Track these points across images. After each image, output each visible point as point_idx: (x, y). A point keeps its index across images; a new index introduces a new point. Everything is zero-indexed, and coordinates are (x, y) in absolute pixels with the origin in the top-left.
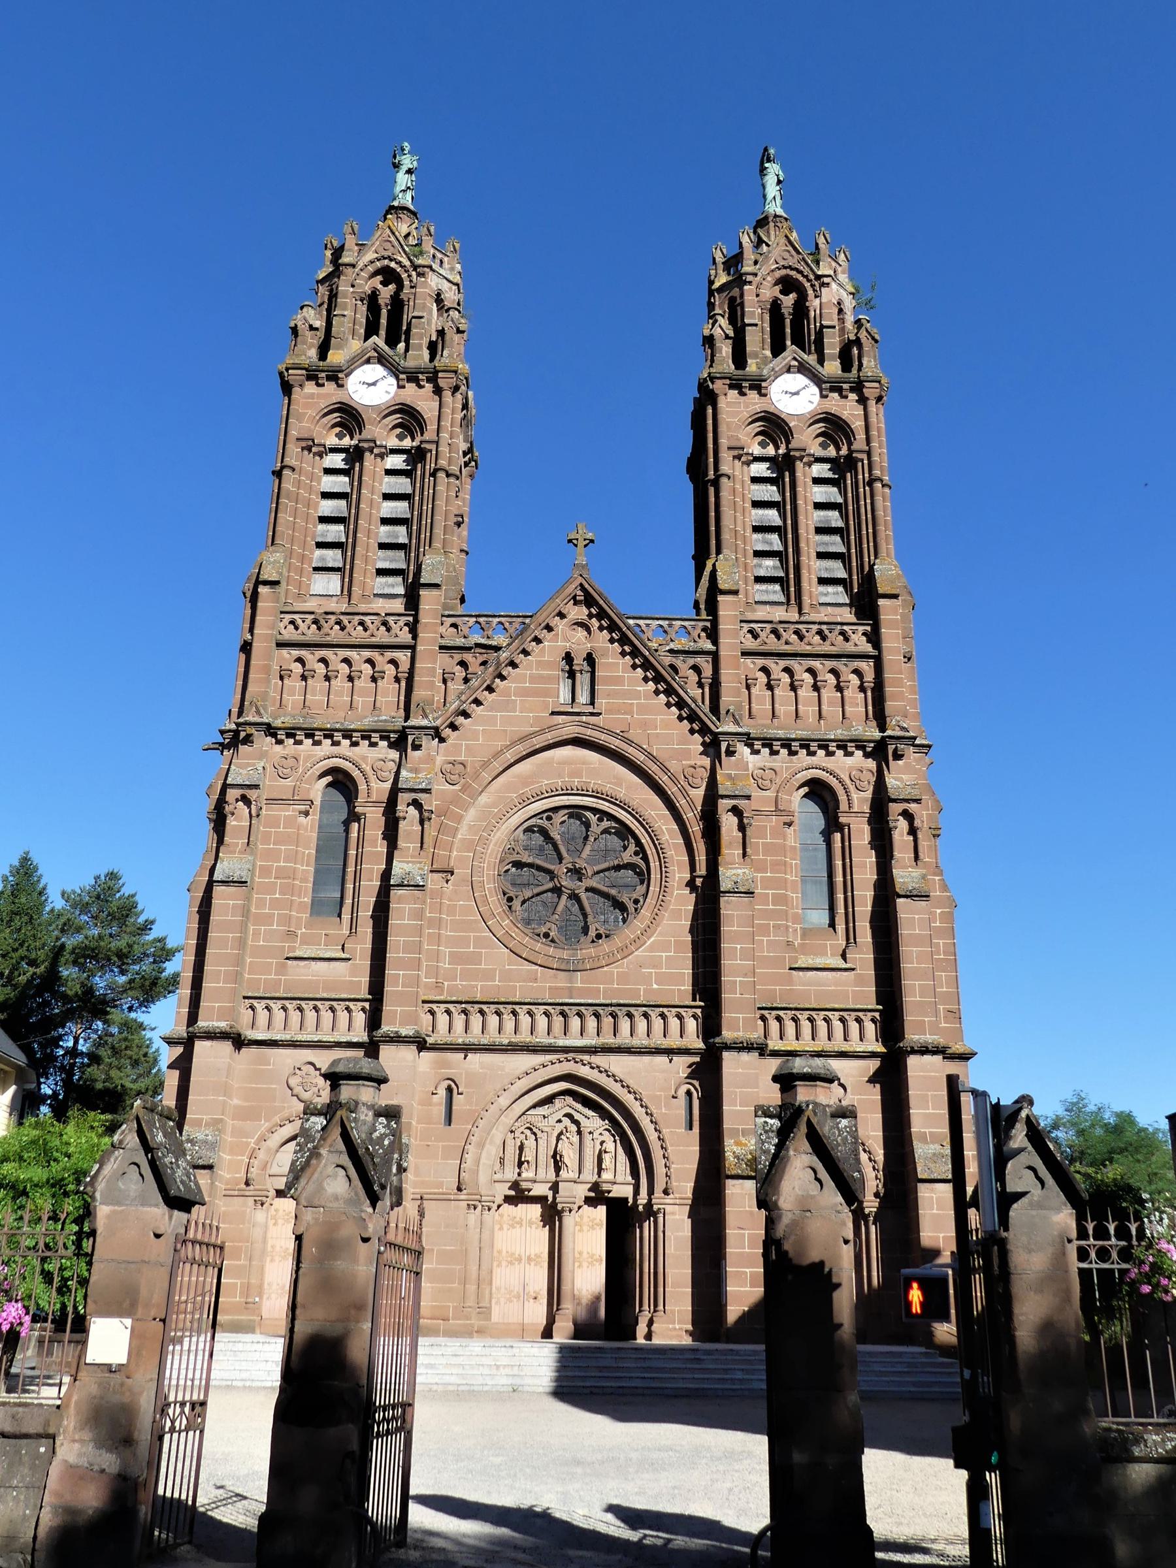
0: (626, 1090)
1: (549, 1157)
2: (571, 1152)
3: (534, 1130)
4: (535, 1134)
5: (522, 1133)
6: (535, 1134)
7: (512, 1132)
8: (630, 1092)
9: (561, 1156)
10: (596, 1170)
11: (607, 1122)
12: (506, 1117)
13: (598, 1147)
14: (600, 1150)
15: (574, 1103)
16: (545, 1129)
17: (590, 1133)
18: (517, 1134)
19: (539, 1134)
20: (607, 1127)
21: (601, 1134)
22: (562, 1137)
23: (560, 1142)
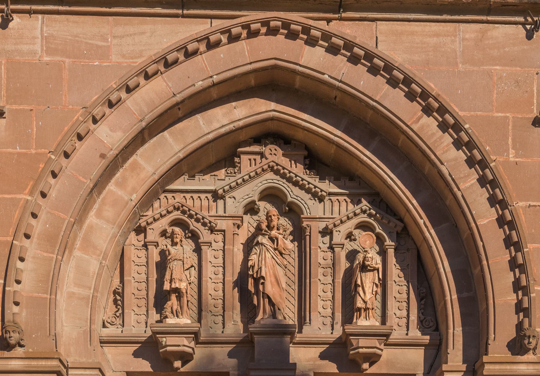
0: (416, 107)
1: (229, 285)
2: (280, 272)
3: (193, 225)
4: (194, 236)
5: (164, 234)
6: (194, 236)
7: (140, 230)
8: (427, 111)
9: (258, 280)
10: (339, 316)
11: (365, 204)
12: (121, 185)
13: (343, 265)
14: (349, 274)
15: (285, 162)
16: (221, 224)
17: (326, 232)
18: (152, 235)
19: (205, 235)
20: (363, 218)
21: (350, 236)
22: (260, 239)
23: (256, 250)
